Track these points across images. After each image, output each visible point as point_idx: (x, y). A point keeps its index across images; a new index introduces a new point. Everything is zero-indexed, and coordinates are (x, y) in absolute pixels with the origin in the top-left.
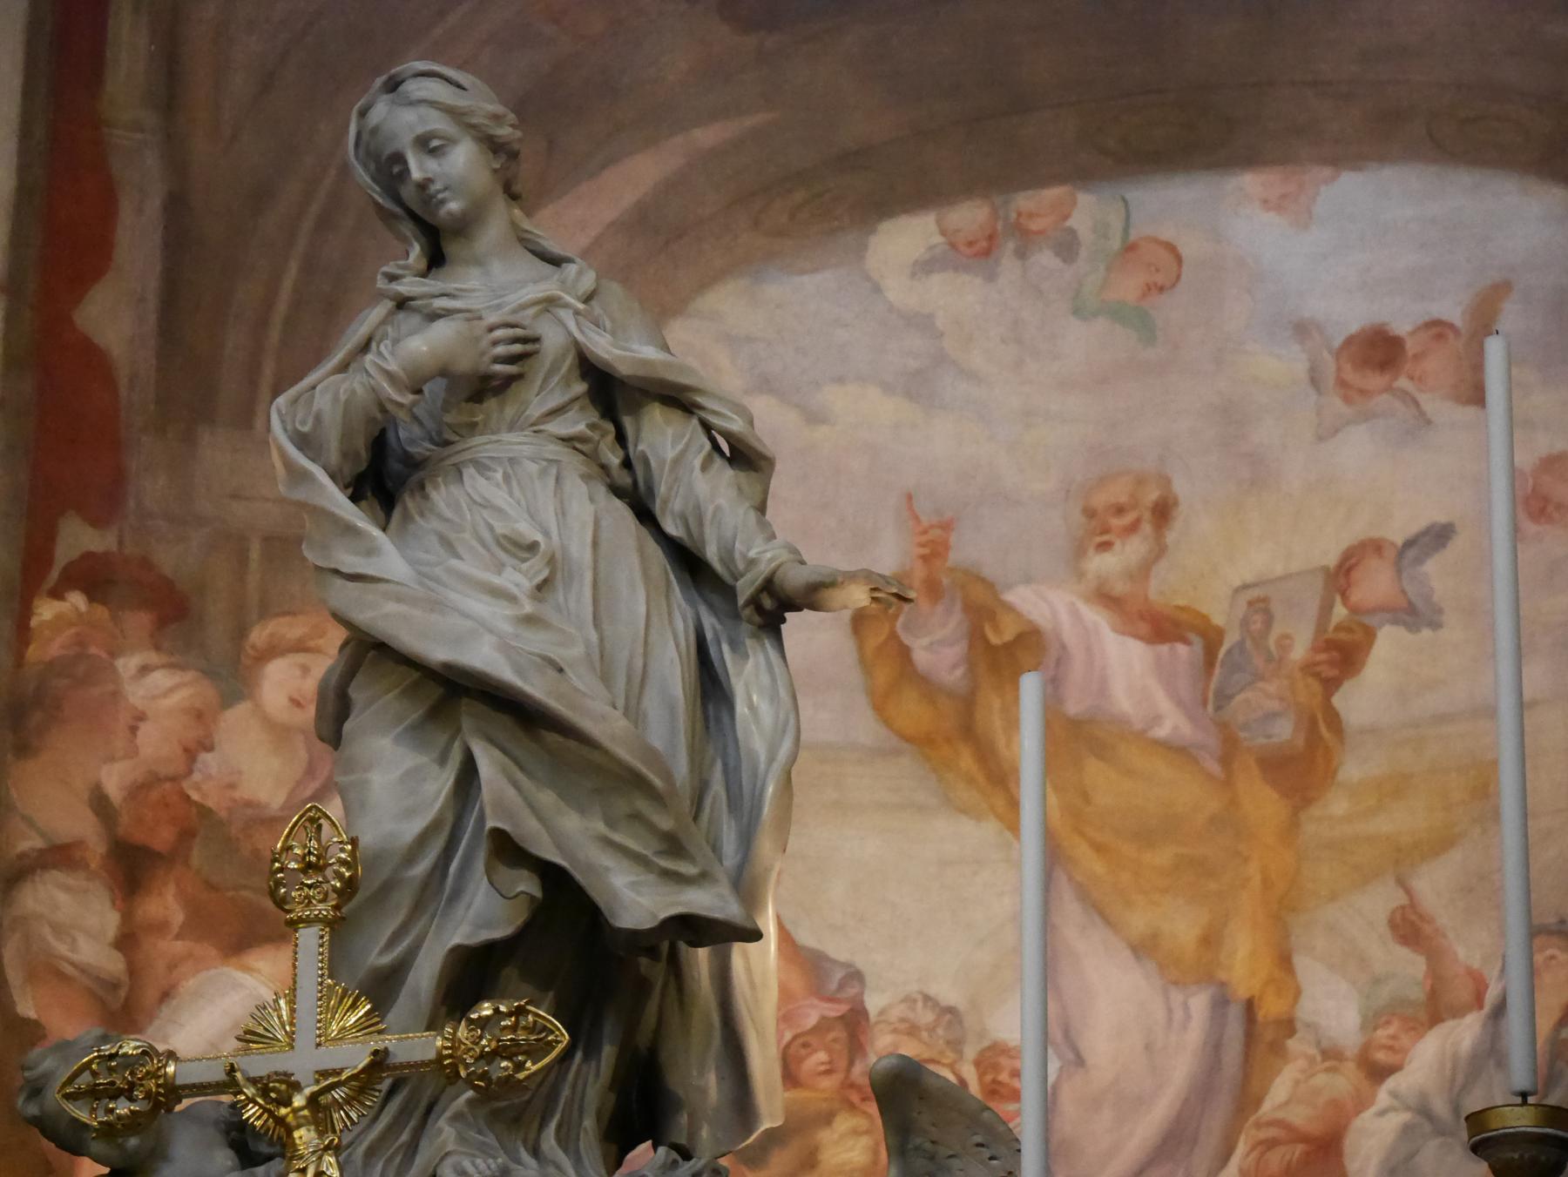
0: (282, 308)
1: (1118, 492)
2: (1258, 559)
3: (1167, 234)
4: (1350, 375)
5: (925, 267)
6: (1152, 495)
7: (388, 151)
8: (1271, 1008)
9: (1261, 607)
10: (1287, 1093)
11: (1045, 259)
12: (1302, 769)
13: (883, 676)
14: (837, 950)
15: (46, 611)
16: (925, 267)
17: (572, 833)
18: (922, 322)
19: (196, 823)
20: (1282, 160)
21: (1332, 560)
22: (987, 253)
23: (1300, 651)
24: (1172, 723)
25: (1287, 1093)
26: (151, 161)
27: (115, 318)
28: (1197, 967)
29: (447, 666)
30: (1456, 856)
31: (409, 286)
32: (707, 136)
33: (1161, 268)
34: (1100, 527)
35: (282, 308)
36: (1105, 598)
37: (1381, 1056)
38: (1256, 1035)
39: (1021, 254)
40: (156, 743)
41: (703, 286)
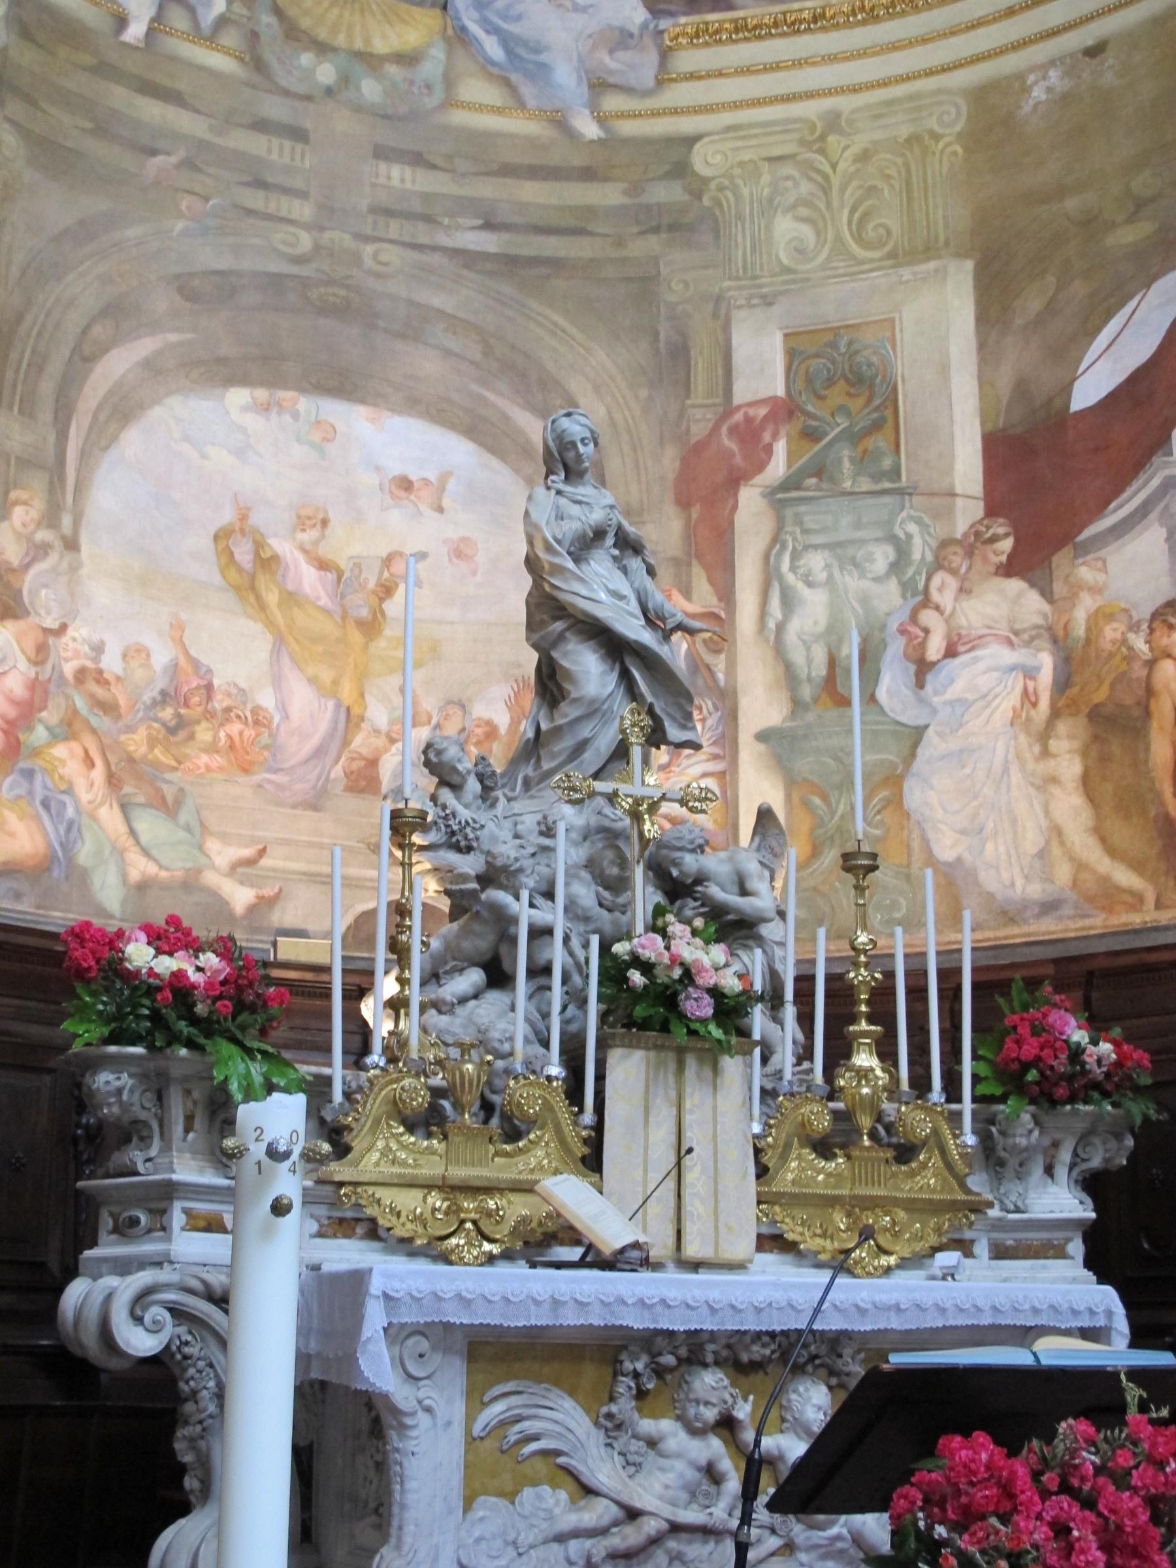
0: (24, 365)
1: (308, 512)
2: (357, 549)
3: (332, 421)
4: (393, 488)
5: (245, 409)
6: (321, 516)
7: (568, 439)
8: (356, 711)
9: (358, 566)
10: (361, 742)
11: (287, 418)
12: (371, 626)
13: (224, 560)
14: (204, 659)
16: (245, 409)
18: (243, 430)
20: (375, 405)
21: (384, 555)
22: (267, 410)
23: (372, 584)
24: (324, 601)
25: (361, 742)
28: (330, 691)
29: (636, 642)
31: (561, 486)
32: (173, 337)
33: (330, 433)
34: (302, 522)
35: (24, 365)
36: (305, 551)
37: (394, 735)
38: (351, 720)
39: (279, 414)
41: (169, 393)
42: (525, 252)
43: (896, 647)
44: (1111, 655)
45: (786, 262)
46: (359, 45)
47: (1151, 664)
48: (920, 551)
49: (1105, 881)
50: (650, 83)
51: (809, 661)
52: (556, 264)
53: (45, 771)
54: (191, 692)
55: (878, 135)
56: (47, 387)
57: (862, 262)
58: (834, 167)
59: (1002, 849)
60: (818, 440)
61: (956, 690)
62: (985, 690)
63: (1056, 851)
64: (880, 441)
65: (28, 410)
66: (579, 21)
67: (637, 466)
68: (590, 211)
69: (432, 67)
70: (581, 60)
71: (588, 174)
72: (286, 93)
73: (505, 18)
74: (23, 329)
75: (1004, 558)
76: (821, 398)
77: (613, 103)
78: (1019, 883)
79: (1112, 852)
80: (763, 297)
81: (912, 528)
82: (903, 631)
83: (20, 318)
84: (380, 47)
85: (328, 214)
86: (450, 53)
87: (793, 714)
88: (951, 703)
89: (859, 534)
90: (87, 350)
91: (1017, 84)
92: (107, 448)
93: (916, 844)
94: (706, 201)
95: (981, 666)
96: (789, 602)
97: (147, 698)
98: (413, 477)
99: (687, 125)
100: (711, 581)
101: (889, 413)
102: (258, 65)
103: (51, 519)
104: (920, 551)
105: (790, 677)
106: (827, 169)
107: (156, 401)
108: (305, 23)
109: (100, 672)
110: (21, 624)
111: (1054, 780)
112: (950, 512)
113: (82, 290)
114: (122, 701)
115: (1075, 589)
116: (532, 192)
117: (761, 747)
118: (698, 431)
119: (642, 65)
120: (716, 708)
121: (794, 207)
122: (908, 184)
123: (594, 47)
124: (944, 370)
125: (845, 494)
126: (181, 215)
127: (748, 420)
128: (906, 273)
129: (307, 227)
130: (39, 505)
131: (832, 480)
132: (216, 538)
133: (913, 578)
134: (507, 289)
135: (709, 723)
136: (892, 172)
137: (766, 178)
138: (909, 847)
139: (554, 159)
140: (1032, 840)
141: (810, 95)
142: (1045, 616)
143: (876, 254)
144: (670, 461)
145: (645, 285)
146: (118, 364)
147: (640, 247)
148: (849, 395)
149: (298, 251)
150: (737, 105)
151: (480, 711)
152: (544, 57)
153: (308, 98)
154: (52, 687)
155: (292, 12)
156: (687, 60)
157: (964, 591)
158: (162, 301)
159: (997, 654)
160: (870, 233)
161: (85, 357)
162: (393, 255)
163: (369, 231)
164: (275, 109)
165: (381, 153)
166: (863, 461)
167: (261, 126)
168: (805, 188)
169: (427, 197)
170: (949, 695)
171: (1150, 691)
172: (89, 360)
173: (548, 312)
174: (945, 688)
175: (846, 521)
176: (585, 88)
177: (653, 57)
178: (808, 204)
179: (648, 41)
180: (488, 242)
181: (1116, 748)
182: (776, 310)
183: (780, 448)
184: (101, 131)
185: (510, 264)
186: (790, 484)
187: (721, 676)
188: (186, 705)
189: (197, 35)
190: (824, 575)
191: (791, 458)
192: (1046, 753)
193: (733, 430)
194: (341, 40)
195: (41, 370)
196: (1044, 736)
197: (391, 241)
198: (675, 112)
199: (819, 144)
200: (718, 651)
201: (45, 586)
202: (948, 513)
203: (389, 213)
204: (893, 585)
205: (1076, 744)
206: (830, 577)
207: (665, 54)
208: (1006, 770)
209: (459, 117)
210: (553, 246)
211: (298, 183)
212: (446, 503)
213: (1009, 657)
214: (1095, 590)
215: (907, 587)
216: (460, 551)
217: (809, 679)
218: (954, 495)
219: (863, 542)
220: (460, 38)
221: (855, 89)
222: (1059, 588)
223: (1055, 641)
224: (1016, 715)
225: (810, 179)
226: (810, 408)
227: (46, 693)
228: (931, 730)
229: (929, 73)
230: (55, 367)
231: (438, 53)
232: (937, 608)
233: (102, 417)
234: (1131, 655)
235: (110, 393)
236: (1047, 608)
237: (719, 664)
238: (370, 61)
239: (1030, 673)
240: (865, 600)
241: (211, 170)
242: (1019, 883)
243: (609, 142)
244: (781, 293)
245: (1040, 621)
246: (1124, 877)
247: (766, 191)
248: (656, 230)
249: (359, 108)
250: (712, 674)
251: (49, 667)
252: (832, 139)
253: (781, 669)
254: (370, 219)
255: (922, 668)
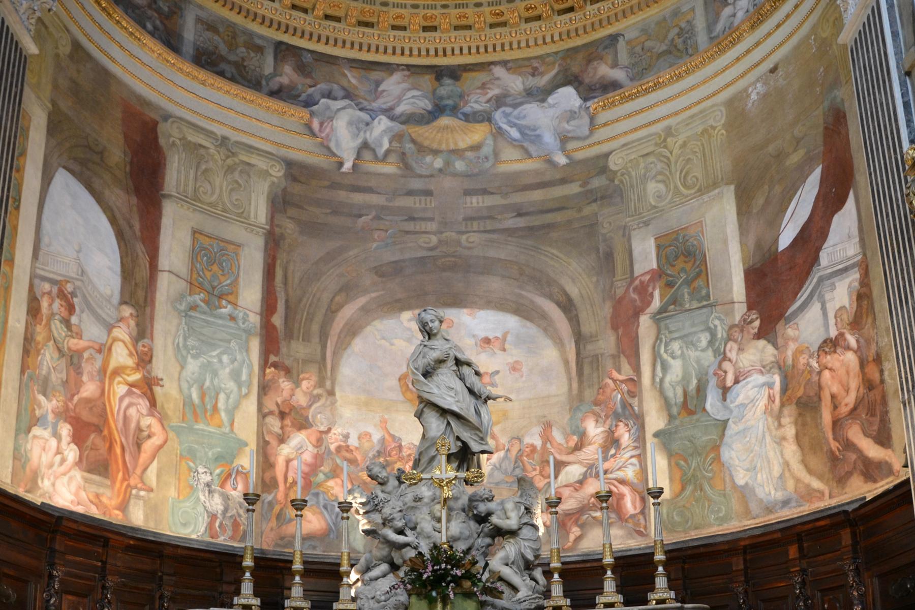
13: (404, 389)
14: (397, 435)
15: (268, 371)
16: (410, 320)
17: (466, 435)
19: (292, 408)
20: (471, 308)
26: (283, 293)
27: (277, 320)
30: (500, 425)
32: (373, 295)
40: (286, 394)
41: (374, 320)
42: (537, 223)
43: (713, 382)
44: (803, 371)
45: (653, 203)
46: (452, 147)
47: (820, 373)
48: (721, 333)
49: (808, 486)
50: (587, 132)
51: (675, 395)
52: (550, 227)
53: (324, 492)
54: (392, 449)
55: (689, 133)
56: (315, 328)
57: (687, 196)
58: (671, 153)
59: (765, 476)
60: (673, 287)
61: (741, 399)
62: (752, 397)
63: (787, 474)
64: (700, 282)
65: (307, 338)
66: (551, 112)
67: (594, 314)
68: (566, 198)
69: (487, 150)
70: (555, 130)
71: (563, 181)
72: (421, 176)
73: (518, 118)
74: (302, 305)
75: (756, 330)
76: (673, 266)
77: (571, 146)
78: (773, 492)
79: (810, 471)
80: (644, 222)
81: (717, 322)
82: (715, 374)
83: (300, 300)
84: (462, 145)
85: (445, 224)
86: (495, 141)
87: (670, 422)
88: (738, 406)
89: (694, 329)
90: (333, 308)
91: (743, 94)
92: (346, 348)
93: (727, 479)
94: (616, 182)
95: (750, 386)
96: (665, 368)
97: (370, 455)
98: (491, 337)
99: (605, 148)
100: (630, 364)
101: (703, 268)
102: (407, 166)
103: (321, 383)
104: (721, 333)
105: (667, 404)
106: (668, 154)
107: (368, 324)
108: (426, 143)
109: (348, 446)
110: (309, 431)
111: (784, 438)
112: (733, 310)
113: (329, 283)
114: (359, 458)
115: (787, 340)
116: (537, 196)
117: (656, 440)
118: (620, 292)
119: (581, 125)
120: (635, 424)
121: (655, 176)
122: (704, 155)
123: (560, 122)
124: (725, 241)
125: (686, 311)
126: (375, 240)
127: (642, 283)
128: (706, 197)
129: (434, 233)
130: (314, 379)
131: (681, 305)
132: (400, 380)
133: (718, 348)
134: (529, 242)
135: (632, 431)
136: (697, 150)
137: (642, 165)
138: (724, 481)
139: (548, 177)
140: (777, 470)
141: (657, 121)
142: (775, 356)
143: (693, 191)
144: (607, 310)
145: (592, 227)
146: (348, 312)
147: (588, 210)
148: (685, 262)
149: (431, 245)
150: (625, 133)
151: (527, 440)
152: (537, 132)
153: (432, 176)
154: (325, 456)
155: (419, 140)
156: (603, 117)
157: (741, 350)
158: (368, 279)
159: (757, 379)
160: (689, 181)
161: (332, 311)
162: (475, 238)
163: (464, 229)
164: (416, 184)
165: (468, 193)
166: (694, 294)
167: (410, 193)
168: (660, 166)
169: (489, 208)
170: (736, 403)
171: (820, 388)
172: (336, 311)
173: (549, 249)
174: (735, 399)
175: (687, 324)
176: (558, 142)
177: (586, 120)
178: (661, 173)
179: (583, 113)
180: (521, 222)
181: (809, 419)
182: (650, 227)
183: (657, 294)
184: (335, 212)
185: (531, 230)
186: (663, 310)
187: (636, 408)
188: (390, 456)
189: (376, 159)
190: (680, 352)
191: (662, 296)
192: (780, 425)
193: (635, 290)
194: (444, 147)
195: (312, 320)
196: (778, 418)
197: (474, 232)
198: (599, 143)
199: (663, 143)
200: (634, 397)
201: (320, 413)
202: (730, 313)
203: (472, 219)
204: (710, 353)
205: (792, 419)
206: (682, 352)
207: (592, 118)
208: (764, 436)
209: (503, 168)
210: (549, 218)
211: (429, 215)
212: (507, 346)
213: (761, 379)
214: (795, 339)
215: (716, 352)
216: (515, 368)
217: (676, 404)
218: (734, 302)
219: (695, 333)
220: (499, 133)
221: (677, 113)
222: (780, 341)
223: (780, 369)
224: (766, 408)
225: (662, 161)
226: (669, 272)
227: (322, 459)
228: (730, 421)
229: (708, 98)
230: (319, 317)
231: (490, 141)
232: (730, 360)
233: (342, 336)
234: (810, 372)
235: (346, 324)
236: (775, 352)
237: (635, 402)
238: (457, 153)
239: (770, 386)
240: (698, 361)
241: (388, 218)
242: (773, 492)
243: (573, 163)
244: (652, 219)
245: (772, 359)
246: (816, 484)
247: (643, 171)
248: (595, 201)
249: (455, 175)
250: (632, 407)
251: (323, 448)
252: (669, 140)
253: (663, 402)
254: (464, 223)
255: (725, 391)
